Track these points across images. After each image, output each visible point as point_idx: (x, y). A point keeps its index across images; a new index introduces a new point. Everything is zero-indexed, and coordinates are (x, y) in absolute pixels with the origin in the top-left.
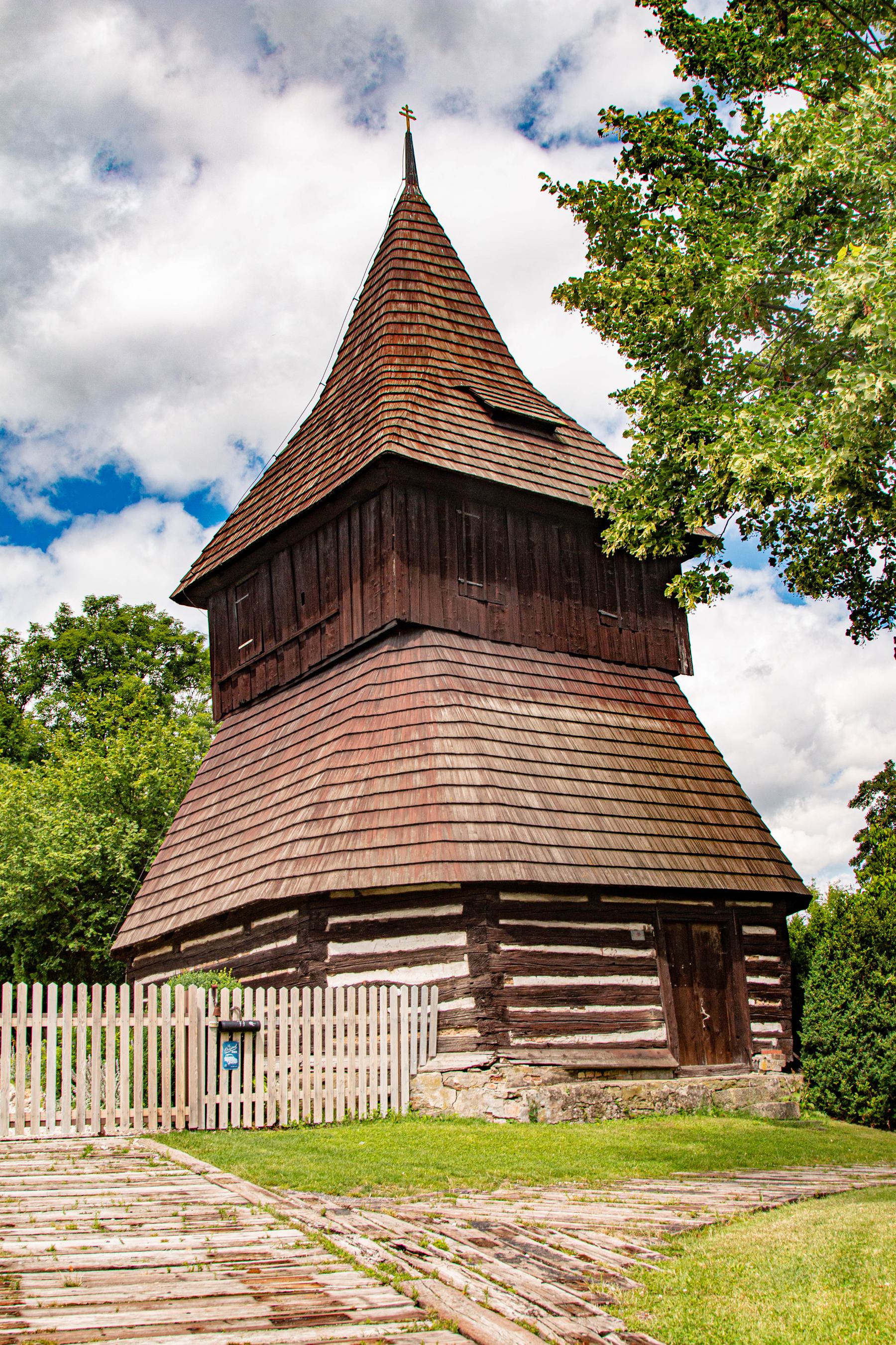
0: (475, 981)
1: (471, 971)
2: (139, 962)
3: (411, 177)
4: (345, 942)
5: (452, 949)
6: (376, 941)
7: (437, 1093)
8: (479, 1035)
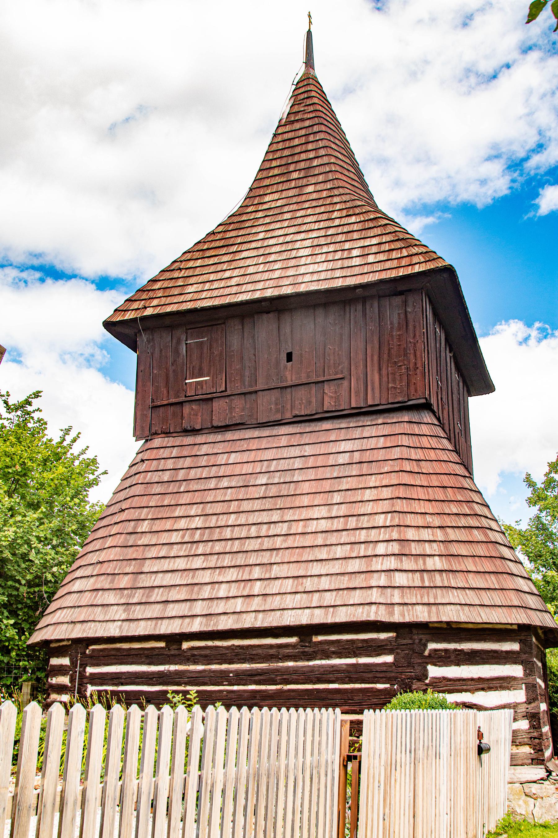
0: (529, 706)
1: (527, 699)
2: (93, 650)
3: (309, 62)
4: (440, 666)
5: (514, 679)
6: (462, 667)
7: (521, 802)
8: (532, 752)
